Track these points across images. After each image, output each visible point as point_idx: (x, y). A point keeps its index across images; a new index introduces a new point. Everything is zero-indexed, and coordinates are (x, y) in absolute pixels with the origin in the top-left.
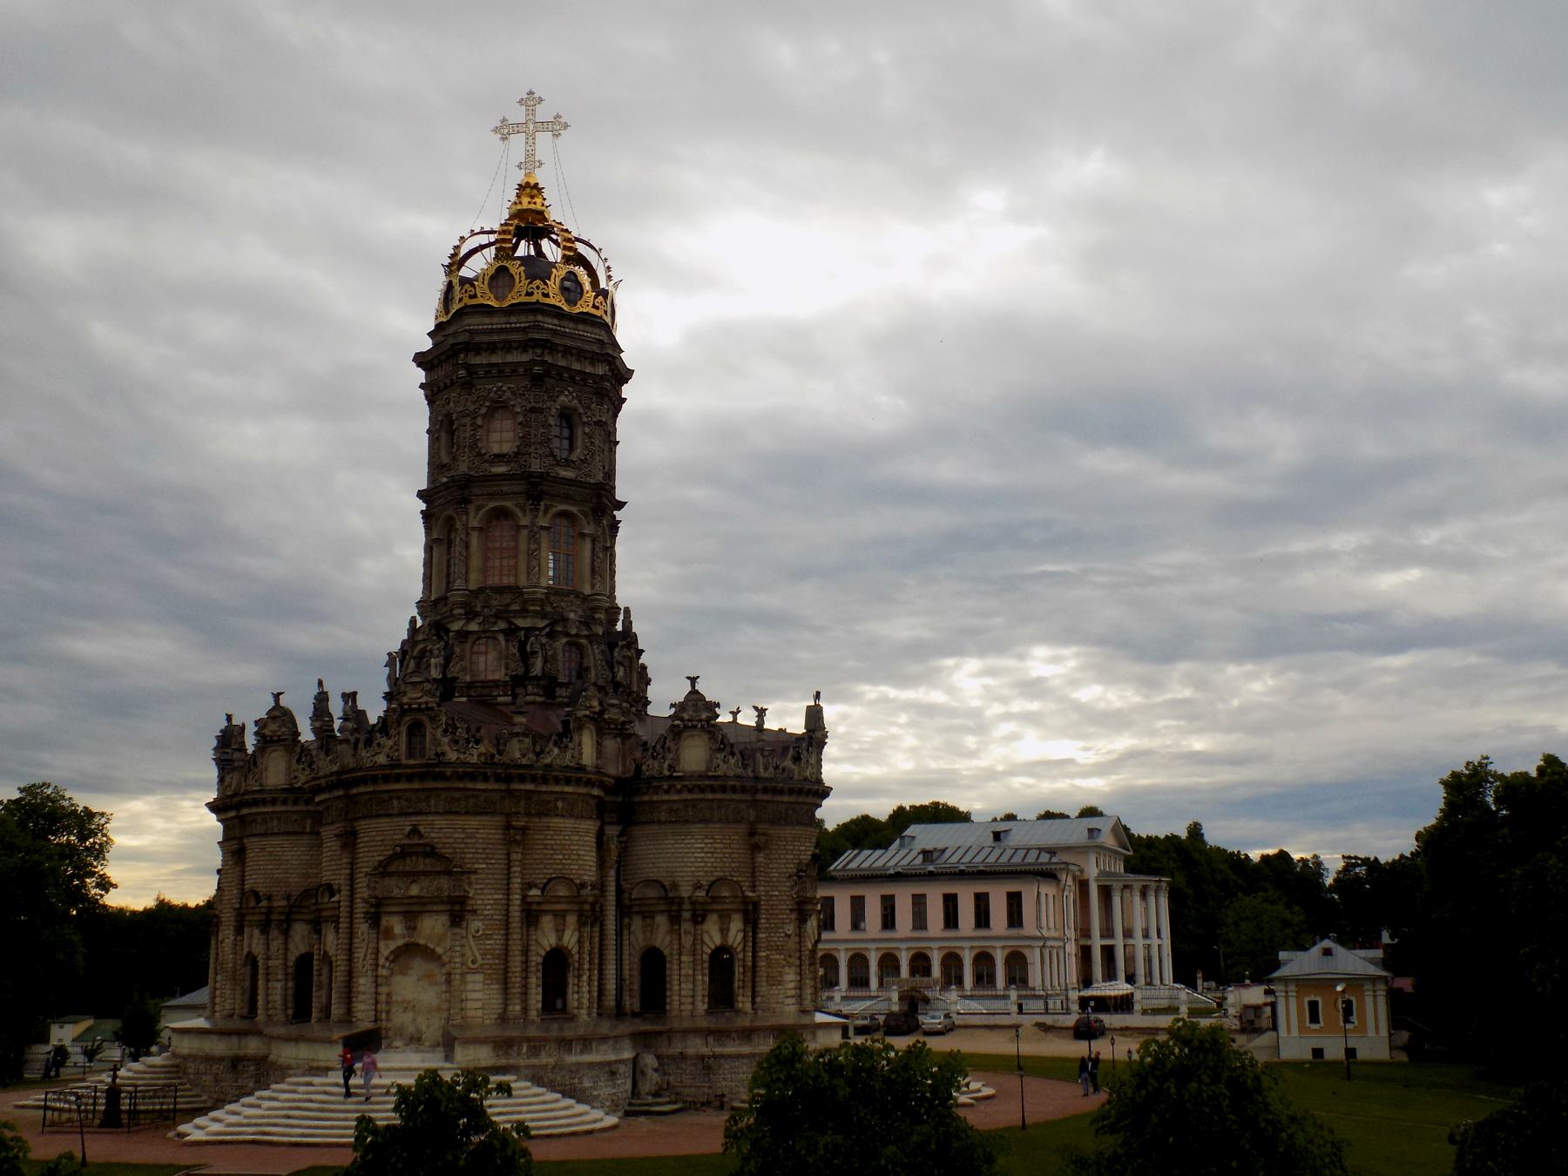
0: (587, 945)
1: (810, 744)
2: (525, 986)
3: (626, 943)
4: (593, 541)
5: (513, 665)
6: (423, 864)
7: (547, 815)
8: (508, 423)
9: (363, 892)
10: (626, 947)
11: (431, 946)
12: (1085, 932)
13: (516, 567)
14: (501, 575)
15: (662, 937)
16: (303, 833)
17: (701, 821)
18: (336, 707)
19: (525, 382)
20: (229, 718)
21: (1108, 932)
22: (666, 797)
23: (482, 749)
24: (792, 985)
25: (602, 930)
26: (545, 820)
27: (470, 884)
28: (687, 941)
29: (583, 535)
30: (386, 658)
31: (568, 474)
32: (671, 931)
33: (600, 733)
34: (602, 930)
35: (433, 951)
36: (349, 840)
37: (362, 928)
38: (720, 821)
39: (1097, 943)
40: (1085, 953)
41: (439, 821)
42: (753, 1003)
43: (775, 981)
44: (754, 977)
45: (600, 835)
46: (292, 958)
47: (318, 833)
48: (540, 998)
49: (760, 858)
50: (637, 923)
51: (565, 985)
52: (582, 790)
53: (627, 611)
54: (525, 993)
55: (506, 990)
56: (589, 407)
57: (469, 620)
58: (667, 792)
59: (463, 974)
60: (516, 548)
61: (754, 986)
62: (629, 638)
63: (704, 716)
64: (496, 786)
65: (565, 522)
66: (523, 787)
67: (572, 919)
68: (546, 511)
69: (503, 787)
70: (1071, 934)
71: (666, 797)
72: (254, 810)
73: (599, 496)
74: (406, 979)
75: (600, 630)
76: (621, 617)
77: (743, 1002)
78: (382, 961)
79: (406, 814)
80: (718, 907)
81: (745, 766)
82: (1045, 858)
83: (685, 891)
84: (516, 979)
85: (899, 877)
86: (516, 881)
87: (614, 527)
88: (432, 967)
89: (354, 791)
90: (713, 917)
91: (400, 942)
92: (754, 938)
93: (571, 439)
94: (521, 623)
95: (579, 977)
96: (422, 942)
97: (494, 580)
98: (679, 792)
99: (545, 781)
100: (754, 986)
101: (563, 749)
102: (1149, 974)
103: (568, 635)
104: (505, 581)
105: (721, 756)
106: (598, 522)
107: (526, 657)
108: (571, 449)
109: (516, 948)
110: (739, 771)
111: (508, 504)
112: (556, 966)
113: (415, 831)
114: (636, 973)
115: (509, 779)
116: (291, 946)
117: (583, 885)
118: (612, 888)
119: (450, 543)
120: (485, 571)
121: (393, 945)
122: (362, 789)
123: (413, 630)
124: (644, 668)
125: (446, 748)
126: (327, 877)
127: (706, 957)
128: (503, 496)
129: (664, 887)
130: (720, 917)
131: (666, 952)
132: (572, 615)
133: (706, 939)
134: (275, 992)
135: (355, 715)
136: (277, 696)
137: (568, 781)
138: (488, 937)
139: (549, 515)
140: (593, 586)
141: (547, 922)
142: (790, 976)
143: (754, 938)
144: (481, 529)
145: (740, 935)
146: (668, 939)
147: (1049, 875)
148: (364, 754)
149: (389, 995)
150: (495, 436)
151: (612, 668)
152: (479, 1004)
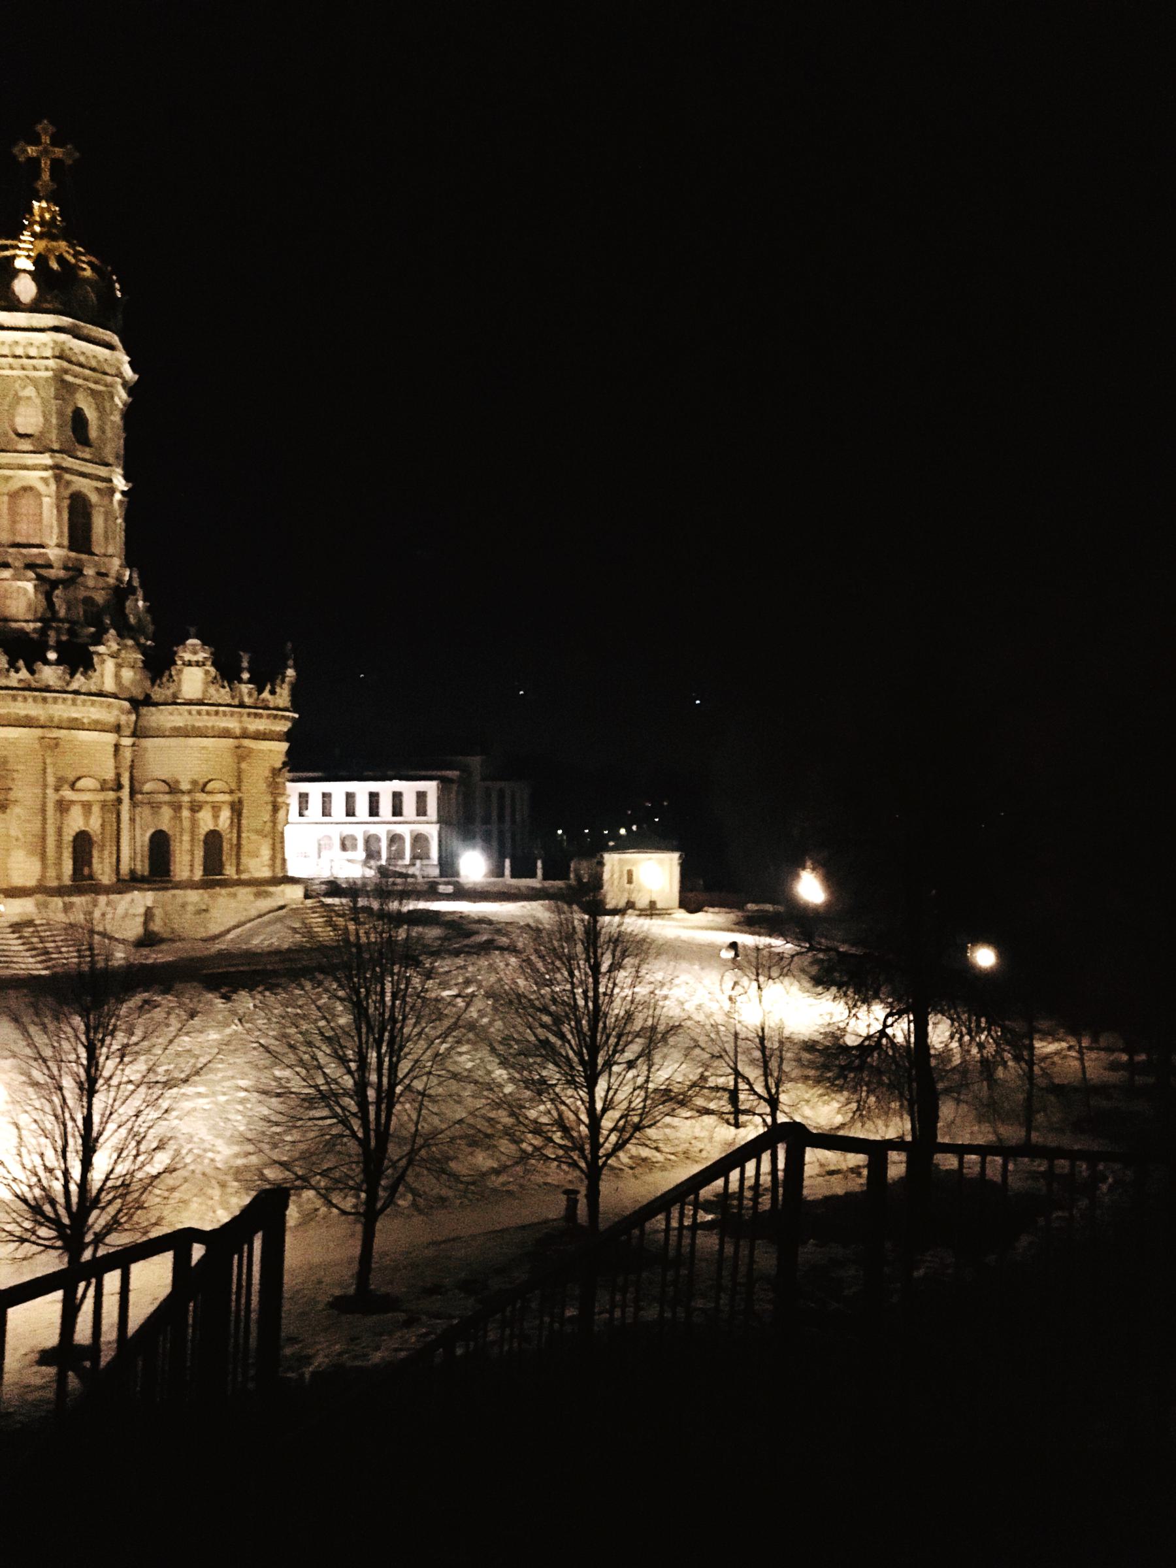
28: (186, 824)
33: (119, 666)
45: (117, 747)
49: (244, 765)
50: (147, 811)
67: (96, 809)
81: (233, 697)
83: (185, 786)
86: (51, 780)
101: (88, 678)
109: (51, 830)
110: (229, 701)
112: (83, 845)
130: (213, 807)
131: (170, 833)
141: (76, 812)
142: (266, 852)
145: (228, 822)
152: (21, 872)
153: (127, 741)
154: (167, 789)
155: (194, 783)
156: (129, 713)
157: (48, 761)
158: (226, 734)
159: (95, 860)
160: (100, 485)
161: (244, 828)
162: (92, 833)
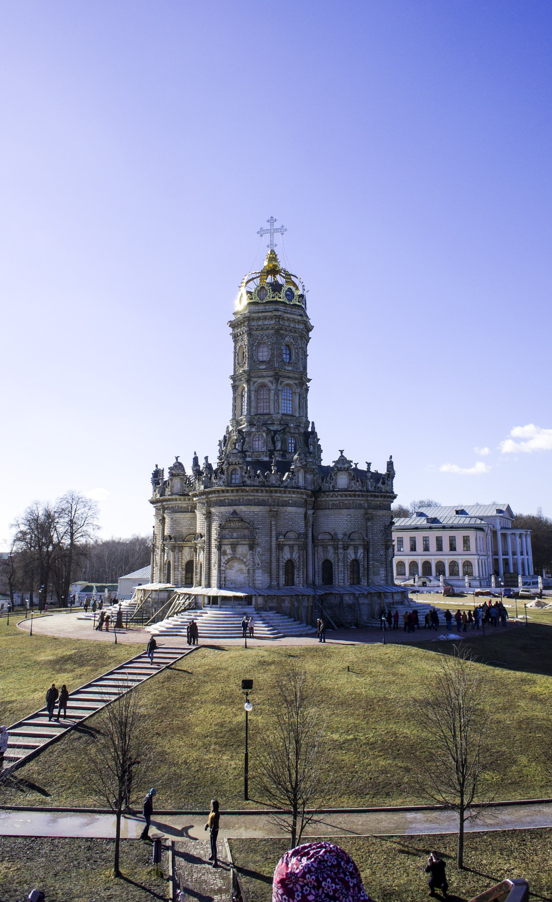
0: (302, 558)
1: (389, 477)
2: (278, 575)
3: (316, 557)
4: (299, 395)
5: (269, 445)
6: (238, 524)
7: (286, 506)
8: (265, 349)
9: (214, 536)
10: (316, 559)
11: (241, 558)
12: (496, 553)
13: (269, 406)
14: (263, 409)
15: (331, 556)
16: (188, 512)
17: (346, 508)
18: (202, 463)
19: (272, 332)
20: (157, 466)
21: (505, 553)
22: (332, 499)
23: (260, 480)
24: (383, 575)
25: (307, 552)
26: (285, 508)
27: (256, 533)
28: (341, 557)
29: (295, 393)
30: (219, 443)
31: (290, 368)
32: (335, 553)
33: (305, 472)
34: (307, 552)
35: (242, 561)
36: (209, 516)
37: (214, 550)
38: (353, 508)
39: (501, 557)
40: (496, 561)
41: (244, 508)
42: (368, 582)
43: (377, 574)
44: (368, 572)
45: (306, 514)
46: (184, 562)
47: (195, 512)
48: (284, 579)
49: (369, 524)
50: (320, 549)
51: (293, 573)
52: (299, 496)
53: (313, 423)
54: (278, 578)
55: (271, 576)
56: (297, 342)
57: (251, 428)
58: (332, 497)
59: (254, 570)
60: (269, 398)
61: (368, 576)
62: (314, 433)
63: (346, 466)
64: (266, 494)
65: (288, 388)
66: (276, 495)
67: (296, 548)
68: (281, 384)
69: (269, 495)
70: (490, 553)
71: (332, 499)
72: (169, 503)
73: (301, 378)
74: (231, 571)
75: (302, 431)
76: (311, 425)
77: (364, 582)
78: (222, 564)
79: (231, 505)
80: (353, 543)
81: (363, 487)
82: (479, 521)
83: (340, 536)
84: (274, 572)
85: (416, 528)
86: (274, 533)
87: (307, 390)
88: (243, 567)
89: (210, 496)
90: (352, 547)
91: (229, 557)
92: (368, 556)
93: (290, 355)
94: (271, 428)
95: (299, 571)
96: (238, 556)
97: (261, 411)
98: (337, 497)
99: (285, 492)
100: (368, 576)
102: (523, 570)
103: (290, 433)
104: (265, 411)
105: (353, 482)
106: (301, 388)
107: (274, 442)
108: (290, 359)
109: (274, 560)
111: (266, 380)
112: (290, 566)
113: (235, 512)
114: (320, 570)
115: (271, 492)
116: (184, 557)
117: (300, 534)
118: (310, 535)
119: (242, 396)
120: (257, 408)
121: (226, 558)
122: (213, 495)
123: (228, 433)
124: (320, 445)
125: (246, 479)
126: (198, 531)
127: (349, 564)
128: (263, 377)
129: (331, 535)
131: (333, 562)
132: (292, 425)
133: (349, 556)
134: (179, 574)
135: (209, 466)
136: (177, 458)
137: (294, 493)
138: (263, 555)
139: (282, 385)
140: (299, 413)
141: (286, 549)
142: (382, 572)
143: (368, 556)
144: (256, 391)
145: (362, 555)
146: (333, 556)
147: (480, 529)
148: (214, 481)
149: (225, 578)
150: (260, 354)
151: (308, 446)
152: (260, 582)
153: (310, 512)
154: (329, 537)
155: (345, 534)
156: (311, 497)
157: (273, 523)
158: (360, 507)
159: (295, 576)
160: (297, 382)
161: (371, 559)
162: (294, 561)
